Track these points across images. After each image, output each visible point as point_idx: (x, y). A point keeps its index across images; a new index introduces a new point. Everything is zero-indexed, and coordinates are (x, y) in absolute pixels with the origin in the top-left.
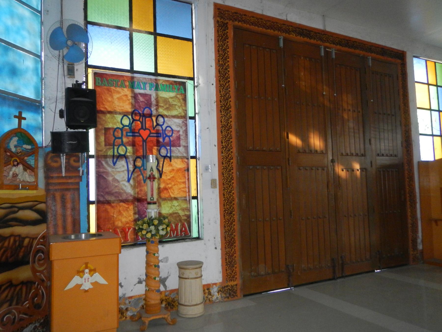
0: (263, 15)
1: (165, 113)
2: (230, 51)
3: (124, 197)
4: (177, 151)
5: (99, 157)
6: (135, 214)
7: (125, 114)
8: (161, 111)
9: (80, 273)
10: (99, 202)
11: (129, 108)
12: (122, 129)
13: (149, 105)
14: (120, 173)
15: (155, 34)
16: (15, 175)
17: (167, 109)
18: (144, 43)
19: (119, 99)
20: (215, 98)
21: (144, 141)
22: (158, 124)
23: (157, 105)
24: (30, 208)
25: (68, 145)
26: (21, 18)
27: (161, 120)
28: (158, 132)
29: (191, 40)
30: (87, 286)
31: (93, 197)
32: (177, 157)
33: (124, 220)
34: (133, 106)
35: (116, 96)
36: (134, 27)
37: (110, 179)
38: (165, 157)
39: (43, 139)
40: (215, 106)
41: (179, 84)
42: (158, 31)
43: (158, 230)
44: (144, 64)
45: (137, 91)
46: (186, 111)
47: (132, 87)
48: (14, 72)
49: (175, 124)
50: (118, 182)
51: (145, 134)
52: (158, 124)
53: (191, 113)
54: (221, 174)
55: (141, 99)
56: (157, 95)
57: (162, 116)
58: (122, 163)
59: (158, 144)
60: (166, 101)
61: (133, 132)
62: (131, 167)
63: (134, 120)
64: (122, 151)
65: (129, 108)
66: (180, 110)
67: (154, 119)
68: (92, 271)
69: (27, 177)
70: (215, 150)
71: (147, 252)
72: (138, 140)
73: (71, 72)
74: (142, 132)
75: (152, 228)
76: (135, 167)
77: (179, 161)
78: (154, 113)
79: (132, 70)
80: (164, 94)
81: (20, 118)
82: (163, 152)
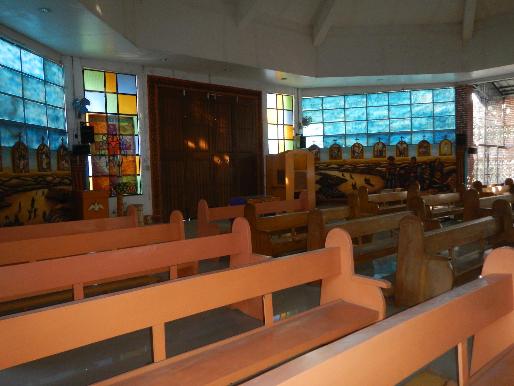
0: (174, 79)
1: (123, 133)
3: (105, 174)
4: (130, 152)
6: (110, 182)
8: (121, 132)
9: (94, 204)
10: (93, 176)
11: (105, 132)
12: (103, 142)
13: (115, 129)
14: (103, 162)
15: (117, 93)
16: (63, 165)
17: (124, 131)
18: (112, 98)
19: (101, 127)
20: (148, 125)
21: (114, 147)
22: (120, 139)
23: (119, 130)
24: (67, 178)
26: (58, 93)
27: (121, 137)
29: (136, 95)
30: (97, 209)
31: (91, 174)
32: (130, 155)
33: (105, 185)
34: (108, 130)
35: (99, 126)
36: (107, 91)
37: (98, 166)
38: (124, 155)
40: (148, 129)
41: (130, 118)
42: (119, 92)
43: (123, 188)
44: (112, 109)
45: (110, 123)
46: (133, 132)
47: (107, 121)
48: (57, 119)
49: (128, 139)
50: (101, 167)
51: (113, 144)
52: (120, 139)
53: (136, 133)
54: (152, 163)
55: (111, 127)
56: (119, 125)
57: (122, 135)
59: (121, 149)
60: (123, 127)
61: (108, 143)
62: (107, 160)
63: (108, 137)
64: (103, 152)
65: (105, 132)
66: (131, 132)
67: (118, 136)
68: (98, 204)
70: (149, 152)
71: (118, 199)
72: (111, 147)
73: (80, 117)
74: (112, 143)
75: (121, 187)
76: (109, 160)
77: (130, 157)
78: (118, 133)
79: (106, 113)
80: (122, 124)
82: (123, 152)
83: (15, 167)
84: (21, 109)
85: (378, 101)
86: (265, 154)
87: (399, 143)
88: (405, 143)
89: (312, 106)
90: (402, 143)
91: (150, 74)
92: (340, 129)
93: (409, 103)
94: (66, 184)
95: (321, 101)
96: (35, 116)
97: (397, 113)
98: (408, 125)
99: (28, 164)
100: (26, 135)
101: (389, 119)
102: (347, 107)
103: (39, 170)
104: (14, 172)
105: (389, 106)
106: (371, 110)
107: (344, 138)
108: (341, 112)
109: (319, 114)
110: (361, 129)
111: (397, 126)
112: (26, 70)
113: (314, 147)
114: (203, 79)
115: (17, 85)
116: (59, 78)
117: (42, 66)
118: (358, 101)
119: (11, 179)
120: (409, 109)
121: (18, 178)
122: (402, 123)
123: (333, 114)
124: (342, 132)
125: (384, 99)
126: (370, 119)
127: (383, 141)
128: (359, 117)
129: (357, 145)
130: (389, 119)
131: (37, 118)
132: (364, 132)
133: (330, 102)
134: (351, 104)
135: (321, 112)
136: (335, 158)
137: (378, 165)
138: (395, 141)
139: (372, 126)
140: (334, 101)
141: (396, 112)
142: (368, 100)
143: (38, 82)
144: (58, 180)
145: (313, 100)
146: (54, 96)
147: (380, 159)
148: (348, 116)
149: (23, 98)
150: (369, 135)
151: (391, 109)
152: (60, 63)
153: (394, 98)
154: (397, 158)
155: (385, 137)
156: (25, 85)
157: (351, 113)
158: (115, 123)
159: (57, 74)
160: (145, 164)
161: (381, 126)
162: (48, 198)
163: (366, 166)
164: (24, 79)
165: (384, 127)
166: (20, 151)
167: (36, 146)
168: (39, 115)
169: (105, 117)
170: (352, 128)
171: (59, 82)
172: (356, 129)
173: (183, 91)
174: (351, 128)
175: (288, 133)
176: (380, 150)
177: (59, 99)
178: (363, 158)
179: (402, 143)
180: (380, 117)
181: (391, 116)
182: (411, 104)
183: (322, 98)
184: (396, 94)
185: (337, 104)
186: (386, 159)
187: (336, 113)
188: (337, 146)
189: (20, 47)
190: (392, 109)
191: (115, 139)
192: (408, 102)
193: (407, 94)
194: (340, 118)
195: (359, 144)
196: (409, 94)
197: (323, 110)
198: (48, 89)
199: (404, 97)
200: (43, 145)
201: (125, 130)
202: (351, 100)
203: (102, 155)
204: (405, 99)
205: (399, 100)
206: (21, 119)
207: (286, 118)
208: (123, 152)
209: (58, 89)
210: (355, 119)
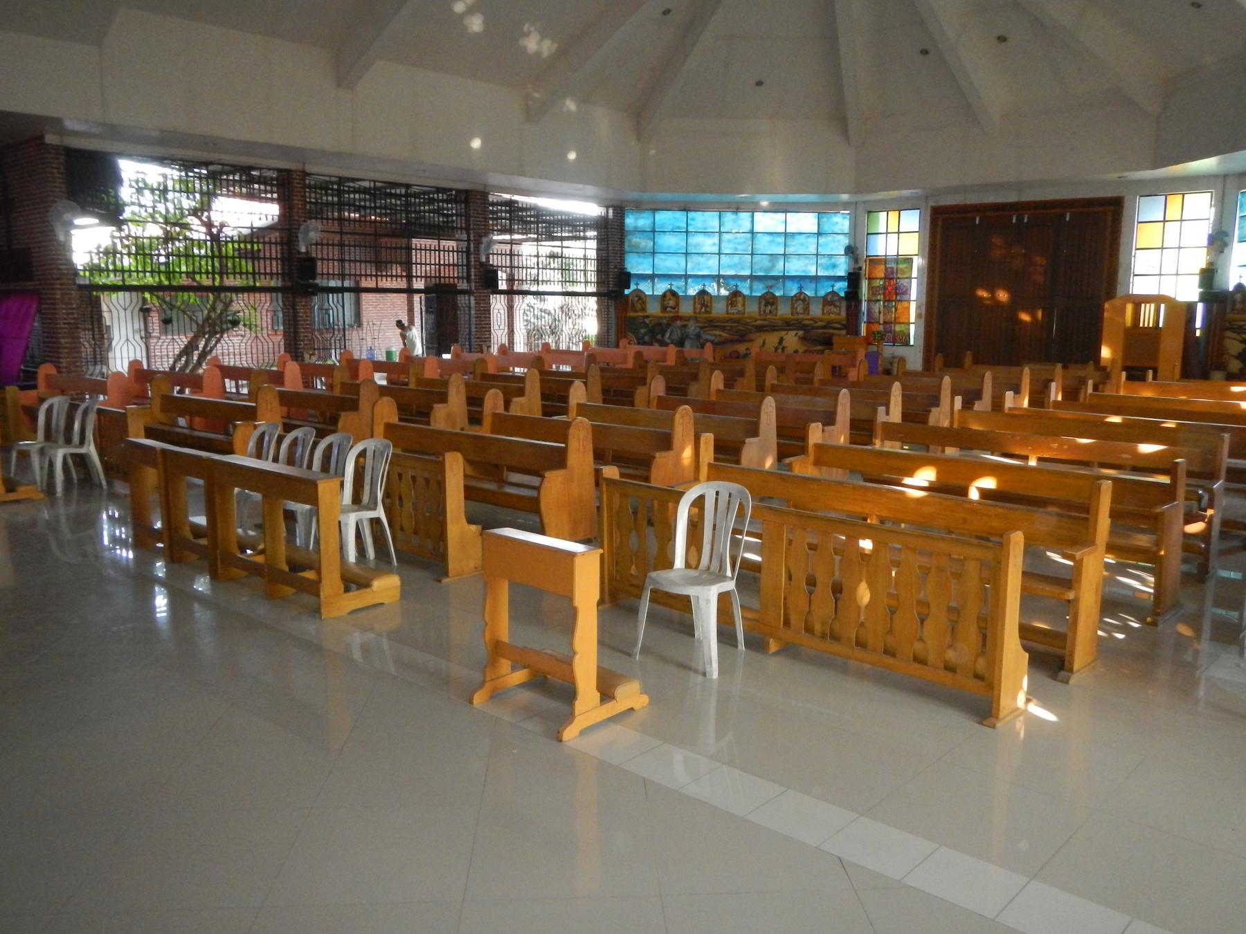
4: (905, 297)
5: (869, 301)
39: (842, 294)
41: (908, 260)
44: (892, 252)
48: (834, 266)
49: (905, 282)
61: (885, 288)
80: (901, 266)
94: (834, 328)
96: (795, 267)
114: (1012, 198)
115: (779, 244)
144: (820, 324)
158: (893, 265)
162: (803, 339)
166: (769, 300)
169: (884, 261)
177: (837, 245)
189: (786, 212)
198: (822, 240)
200: (801, 293)
201: (903, 272)
207: (1200, 232)
209: (841, 237)
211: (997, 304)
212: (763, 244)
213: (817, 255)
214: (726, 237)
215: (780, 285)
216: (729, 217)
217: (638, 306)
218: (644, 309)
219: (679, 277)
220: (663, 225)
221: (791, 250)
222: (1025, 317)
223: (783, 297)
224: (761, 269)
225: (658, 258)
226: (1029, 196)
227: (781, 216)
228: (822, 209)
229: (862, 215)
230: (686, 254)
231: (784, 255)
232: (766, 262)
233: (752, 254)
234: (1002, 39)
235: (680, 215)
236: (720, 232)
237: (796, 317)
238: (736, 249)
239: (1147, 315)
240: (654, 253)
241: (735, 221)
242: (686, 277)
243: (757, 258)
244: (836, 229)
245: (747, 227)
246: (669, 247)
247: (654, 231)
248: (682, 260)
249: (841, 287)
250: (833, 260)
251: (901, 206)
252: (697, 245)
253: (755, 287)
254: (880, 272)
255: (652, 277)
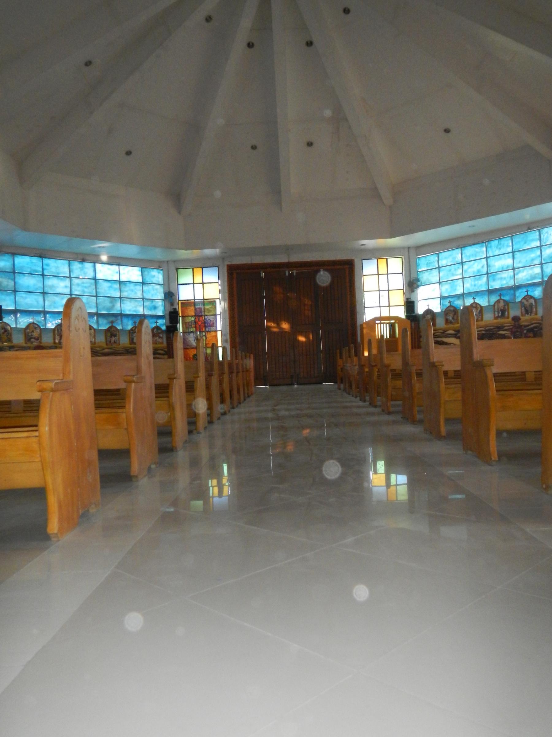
2: (235, 285)
4: (212, 329)
5: (184, 332)
7: (192, 316)
8: (206, 313)
11: (193, 314)
13: (201, 312)
23: (204, 311)
24: (162, 350)
25: (172, 329)
26: (157, 289)
27: (206, 317)
28: (205, 322)
34: (195, 313)
35: (189, 310)
38: (208, 331)
39: (164, 328)
41: (212, 302)
44: (199, 297)
45: (197, 307)
47: (195, 306)
48: (155, 308)
49: (211, 318)
51: (200, 323)
54: (231, 337)
58: (192, 335)
60: (208, 309)
61: (195, 322)
65: (193, 314)
69: (160, 340)
72: (197, 325)
79: (194, 300)
80: (207, 307)
81: (157, 322)
82: (207, 329)
83: (108, 342)
84: (119, 304)
85: (500, 249)
86: (358, 324)
87: (524, 298)
88: (531, 297)
89: (428, 264)
90: (528, 297)
91: (229, 263)
92: (458, 288)
93: (538, 244)
95: (437, 258)
96: (129, 308)
97: (524, 261)
98: (538, 274)
99: (119, 339)
100: (122, 321)
101: (514, 269)
102: (464, 260)
103: (130, 344)
104: (107, 344)
105: (513, 252)
106: (491, 261)
107: (462, 298)
108: (458, 268)
109: (435, 272)
110: (481, 285)
111: (523, 276)
112: (123, 279)
113: (429, 312)
114: (282, 259)
115: (115, 289)
116: (158, 278)
117: (140, 273)
118: (477, 252)
119: (104, 349)
120: (538, 253)
121: (109, 349)
122: (531, 272)
123: (450, 270)
124: (460, 291)
125: (507, 245)
126: (492, 272)
127: (507, 298)
128: (479, 271)
129: (474, 305)
130: (514, 269)
131: (134, 309)
132: (484, 288)
133: (448, 257)
134: (470, 256)
135: (437, 270)
136: (451, 323)
137: (500, 328)
138: (520, 295)
139: (494, 280)
140: (450, 256)
141: (521, 259)
142: (488, 249)
143: (136, 285)
145: (428, 258)
146: (152, 292)
147: (500, 320)
148: (466, 271)
149: (120, 298)
150: (490, 292)
151: (515, 256)
152: (160, 268)
153: (520, 241)
154: (523, 318)
155: (509, 291)
156: (123, 289)
157: (470, 267)
159: (157, 276)
160: (225, 338)
161: (505, 279)
163: (486, 330)
164: (121, 285)
165: (508, 280)
167: (129, 327)
168: (136, 307)
170: (471, 285)
171: (158, 281)
172: (475, 285)
173: (260, 273)
174: (470, 286)
175: (399, 299)
176: (502, 309)
177: (158, 293)
178: (482, 320)
179: (528, 297)
180: (503, 268)
181: (516, 266)
182: (541, 246)
183: (438, 254)
184: (522, 236)
185: (454, 258)
186: (510, 319)
187: (453, 270)
188: (452, 309)
189: (119, 265)
190: (517, 255)
191: (201, 319)
192: (538, 244)
193: (534, 235)
194: (457, 275)
195: (477, 304)
196: (537, 233)
197: (439, 268)
198: (146, 288)
199: (531, 238)
201: (209, 311)
202: (469, 251)
203: (193, 332)
204: (533, 240)
205: (525, 243)
206: (118, 311)
207: (398, 282)
208: (207, 329)
209: (158, 287)
210: (474, 274)
211: (282, 332)
212: (104, 288)
213: (143, 299)
214: (75, 281)
215: (120, 322)
216: (76, 265)
217: (4, 337)
218: (10, 340)
219: (38, 313)
220: (22, 268)
221: (124, 294)
222: (302, 339)
223: (122, 330)
224: (104, 308)
225: (19, 296)
226: (296, 258)
227: (115, 268)
228: (144, 264)
229: (171, 269)
230: (44, 293)
231: (120, 298)
232: (107, 303)
233: (96, 296)
234: (310, 144)
235: (36, 261)
236: (70, 277)
237: (132, 346)
238: (83, 291)
239: (383, 331)
240: (15, 291)
241: (82, 269)
242: (45, 313)
243: (100, 300)
244: (154, 280)
245: (91, 275)
246: (28, 287)
247: (14, 272)
248: (40, 298)
249: (162, 324)
250: (154, 303)
251: (203, 264)
252: (52, 287)
253: (100, 322)
254: (191, 311)
255: (15, 312)
